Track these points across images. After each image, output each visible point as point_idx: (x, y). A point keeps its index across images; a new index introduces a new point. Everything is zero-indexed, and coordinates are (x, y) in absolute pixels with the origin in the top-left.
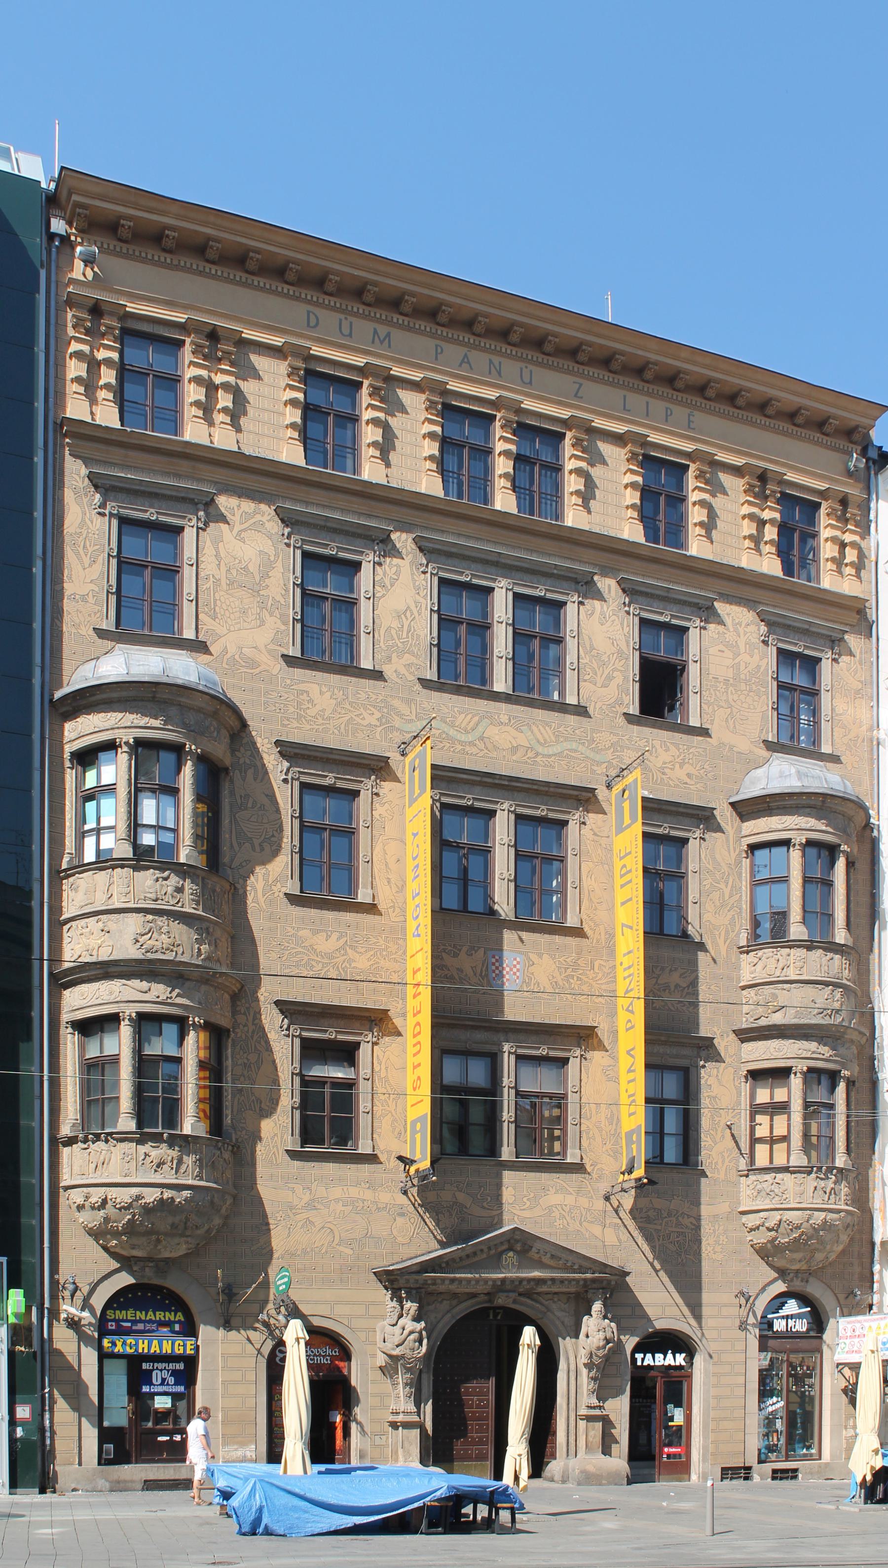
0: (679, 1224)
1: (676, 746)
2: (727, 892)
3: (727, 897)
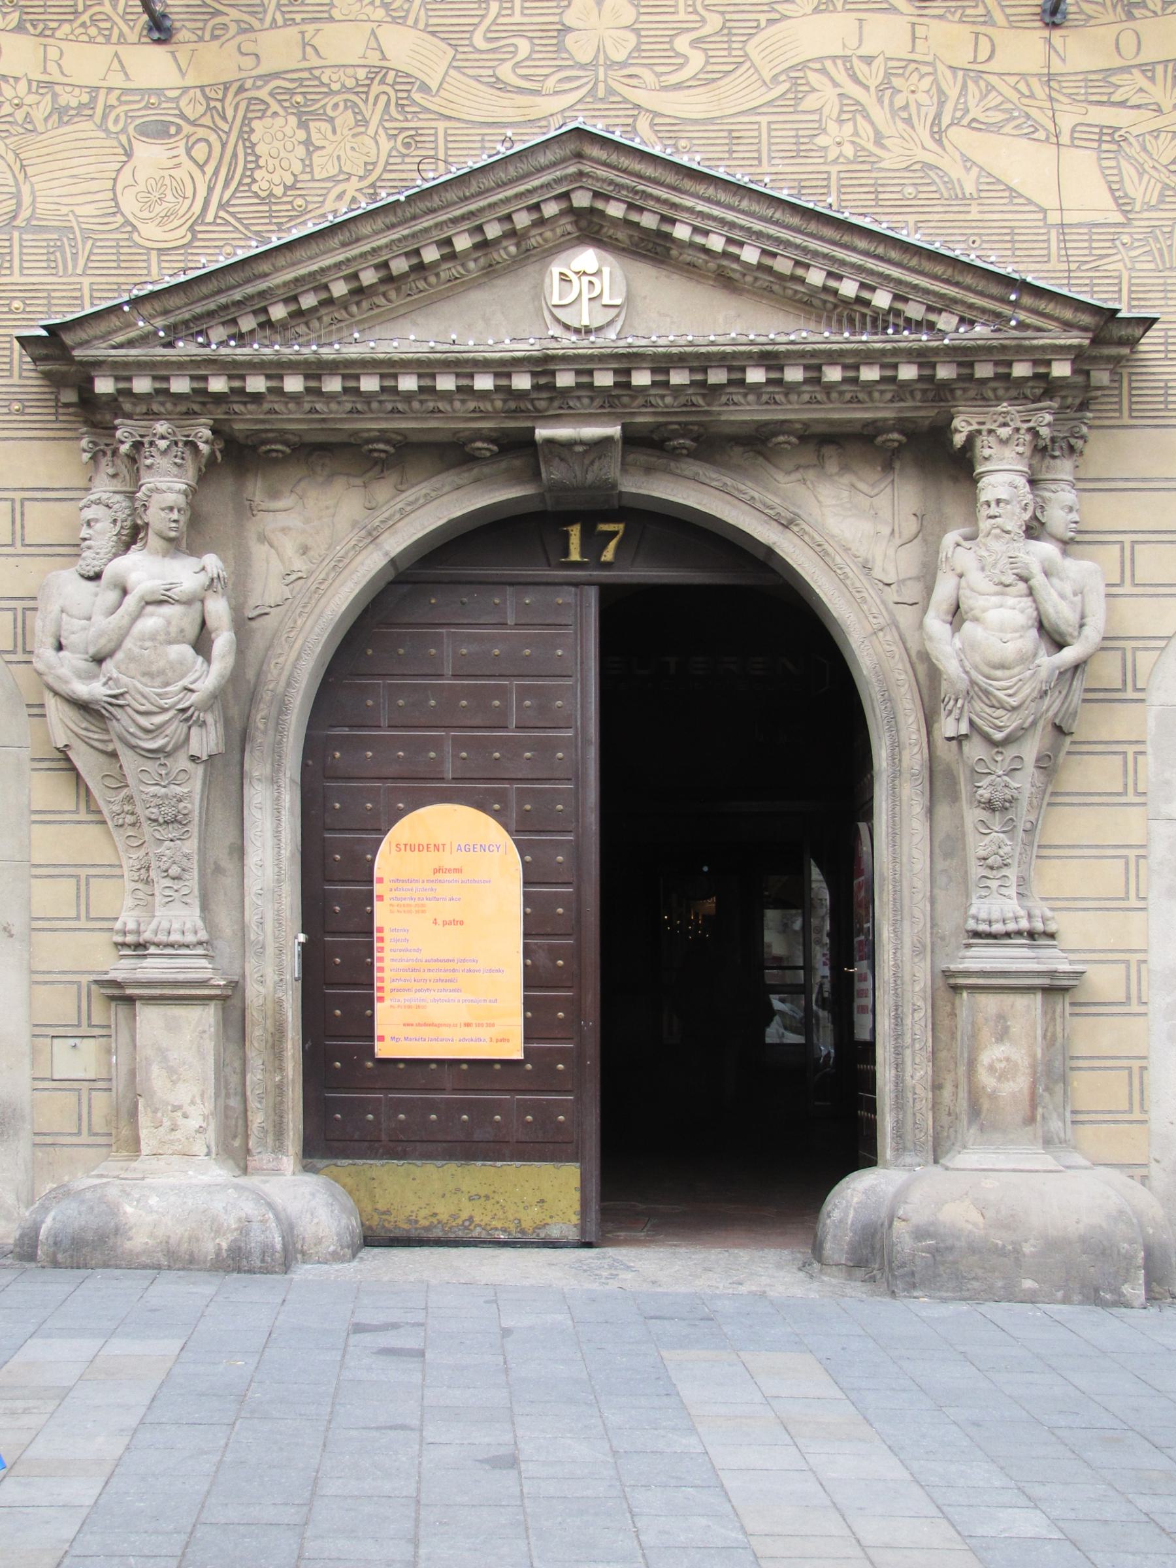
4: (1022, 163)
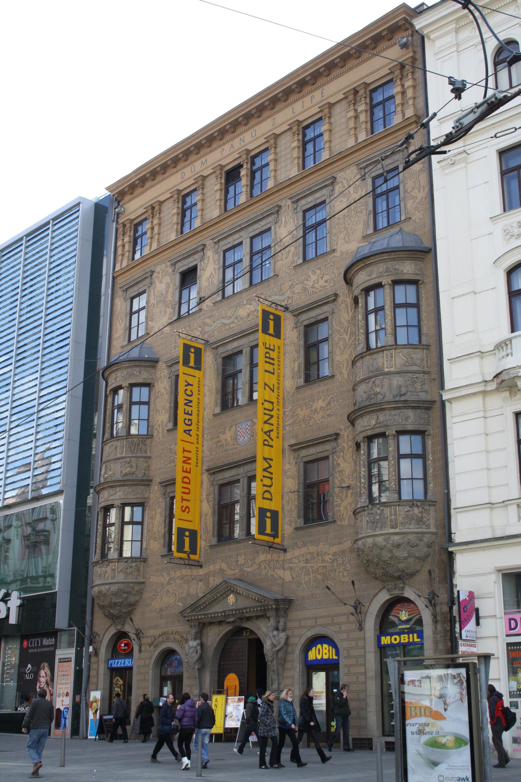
0: (323, 561)
1: (319, 269)
2: (347, 338)
3: (347, 341)
4: (280, 572)
